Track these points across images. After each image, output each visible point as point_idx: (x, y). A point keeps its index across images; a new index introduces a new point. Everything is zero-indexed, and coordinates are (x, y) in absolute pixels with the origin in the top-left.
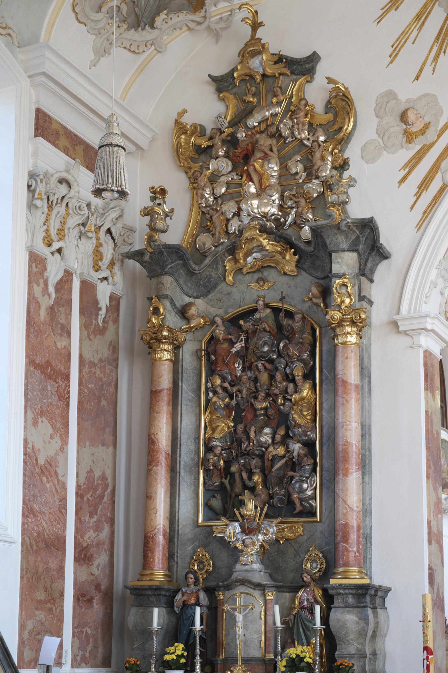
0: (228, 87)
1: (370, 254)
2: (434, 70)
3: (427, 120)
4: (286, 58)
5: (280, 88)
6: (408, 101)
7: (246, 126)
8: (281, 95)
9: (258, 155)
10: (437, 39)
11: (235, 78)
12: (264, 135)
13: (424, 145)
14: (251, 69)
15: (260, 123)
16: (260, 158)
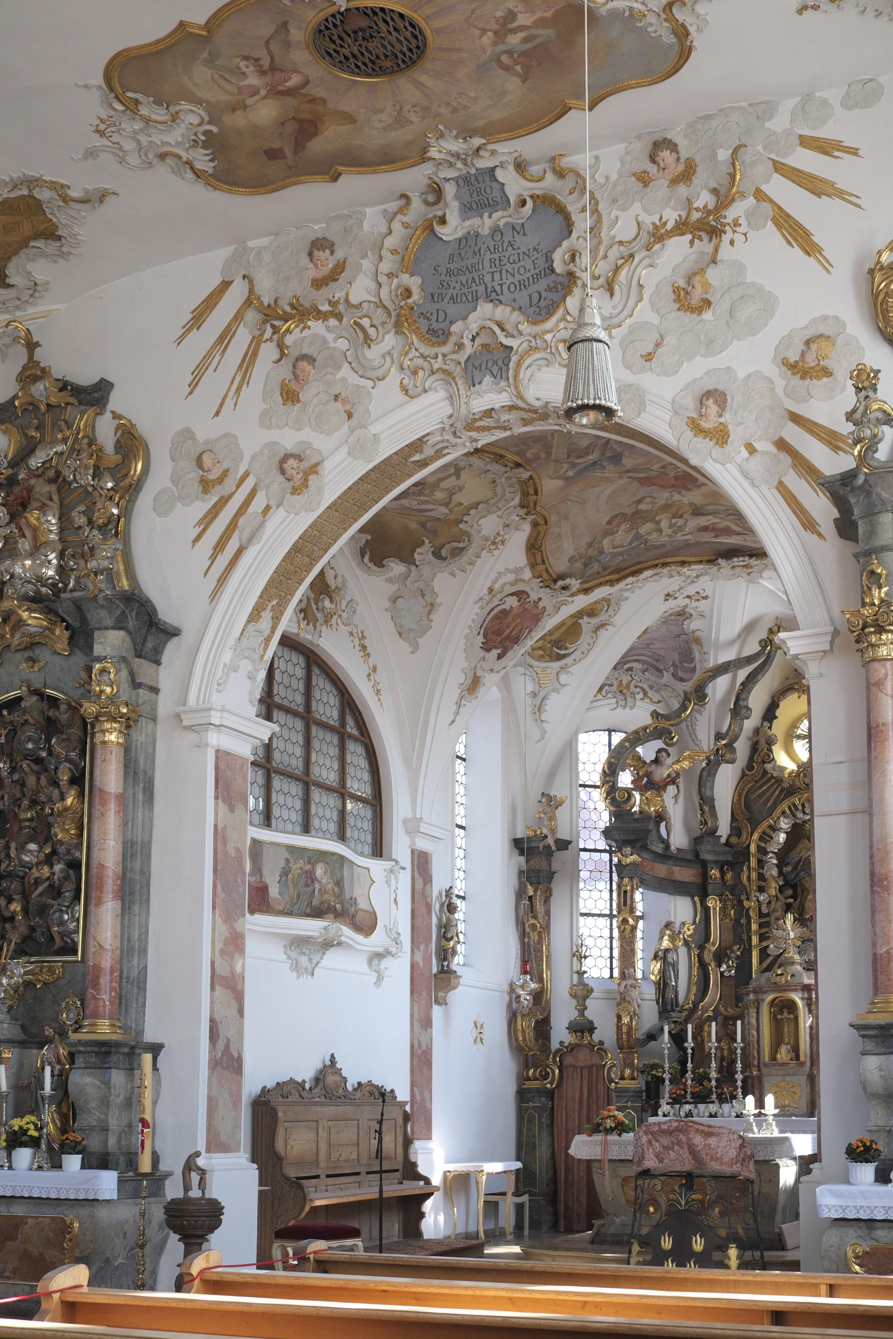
0: (10, 418)
1: (148, 630)
2: (235, 405)
3: (225, 465)
4: (71, 384)
5: (66, 422)
6: (207, 442)
7: (29, 468)
8: (66, 430)
9: (35, 504)
10: (241, 366)
11: (16, 408)
12: (41, 480)
13: (222, 497)
14: (34, 397)
15: (43, 463)
16: (36, 509)
